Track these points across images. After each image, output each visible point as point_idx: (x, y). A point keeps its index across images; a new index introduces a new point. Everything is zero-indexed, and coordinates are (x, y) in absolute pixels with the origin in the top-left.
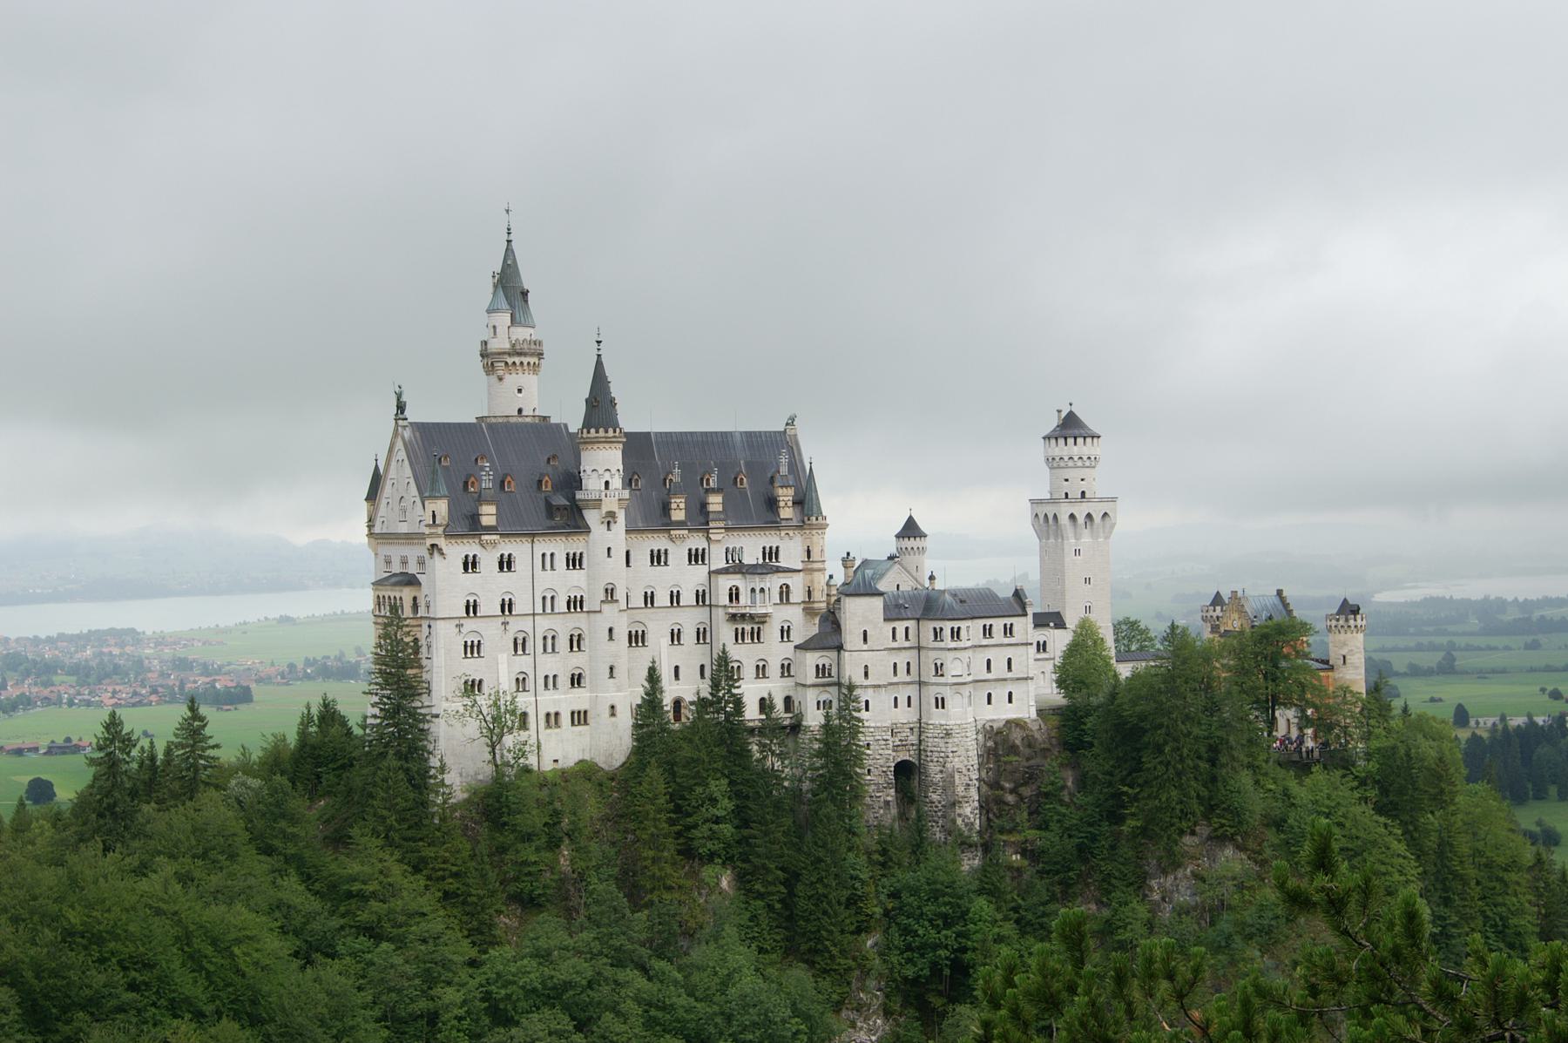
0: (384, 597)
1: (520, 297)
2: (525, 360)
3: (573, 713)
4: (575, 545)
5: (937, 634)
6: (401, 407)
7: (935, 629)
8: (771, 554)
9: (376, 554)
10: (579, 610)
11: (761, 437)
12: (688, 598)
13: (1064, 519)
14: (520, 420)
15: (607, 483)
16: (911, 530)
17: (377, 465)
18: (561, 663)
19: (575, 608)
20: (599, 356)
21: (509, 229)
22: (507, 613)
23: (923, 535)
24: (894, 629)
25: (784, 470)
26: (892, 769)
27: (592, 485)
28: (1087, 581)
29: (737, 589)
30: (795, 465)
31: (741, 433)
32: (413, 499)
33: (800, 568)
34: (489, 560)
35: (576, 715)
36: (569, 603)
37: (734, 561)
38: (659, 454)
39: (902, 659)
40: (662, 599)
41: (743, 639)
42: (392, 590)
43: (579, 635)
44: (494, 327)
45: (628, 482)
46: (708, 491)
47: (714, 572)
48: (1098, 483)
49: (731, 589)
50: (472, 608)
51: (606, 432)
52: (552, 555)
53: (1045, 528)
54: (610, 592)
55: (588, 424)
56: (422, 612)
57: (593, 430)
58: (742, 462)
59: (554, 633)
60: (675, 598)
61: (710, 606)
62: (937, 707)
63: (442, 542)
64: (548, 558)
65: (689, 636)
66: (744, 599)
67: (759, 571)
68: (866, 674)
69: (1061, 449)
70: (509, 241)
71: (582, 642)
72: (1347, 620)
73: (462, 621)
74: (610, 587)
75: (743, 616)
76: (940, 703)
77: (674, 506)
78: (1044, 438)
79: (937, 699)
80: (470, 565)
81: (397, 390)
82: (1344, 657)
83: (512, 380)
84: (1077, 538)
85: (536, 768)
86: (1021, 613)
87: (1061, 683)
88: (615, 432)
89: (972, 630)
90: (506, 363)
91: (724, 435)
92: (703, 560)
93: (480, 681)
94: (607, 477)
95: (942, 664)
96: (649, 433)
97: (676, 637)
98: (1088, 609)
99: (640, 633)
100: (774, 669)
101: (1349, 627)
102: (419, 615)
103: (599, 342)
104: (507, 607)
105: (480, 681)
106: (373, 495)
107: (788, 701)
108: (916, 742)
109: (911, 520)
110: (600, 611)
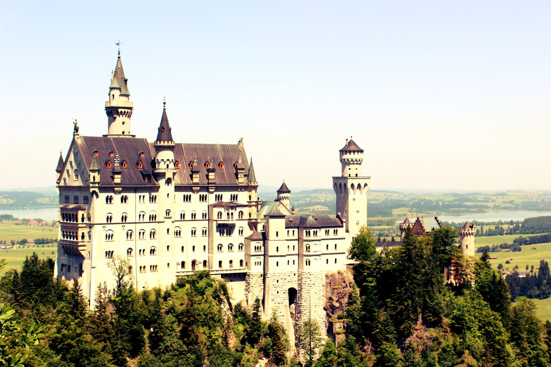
0: (66, 214)
1: (123, 82)
2: (126, 110)
3: (151, 266)
4: (153, 194)
5: (308, 234)
6: (76, 129)
7: (306, 231)
8: (234, 197)
9: (60, 195)
10: (154, 221)
11: (228, 146)
12: (199, 216)
13: (349, 186)
14: (124, 137)
15: (168, 165)
16: (283, 189)
17: (61, 156)
18: (147, 243)
19: (152, 220)
20: (164, 109)
21: (119, 52)
22: (124, 222)
23: (289, 192)
24: (288, 231)
25: (240, 161)
26: (288, 291)
27: (161, 167)
28: (358, 212)
29: (221, 213)
30: (244, 161)
31: (220, 145)
32: (82, 171)
33: (247, 204)
34: (117, 198)
35: (152, 267)
36: (150, 218)
37: (218, 200)
38: (185, 152)
39: (291, 244)
40: (188, 217)
41: (223, 235)
42: (71, 211)
43: (154, 232)
44: (113, 95)
45: (176, 164)
46: (209, 171)
47: (211, 205)
48: (361, 170)
49: (218, 213)
50: (109, 219)
51: (168, 143)
52: (144, 196)
53: (339, 189)
54: (168, 212)
55: (159, 139)
56: (86, 221)
57: (162, 142)
58: (221, 157)
59: (143, 231)
60: (194, 216)
61: (208, 220)
62: (307, 265)
63: (97, 190)
64: (142, 198)
65: (199, 233)
66: (225, 216)
67: (231, 205)
68: (277, 250)
69: (347, 156)
70: (119, 57)
71: (155, 235)
72: (469, 230)
73: (105, 225)
74: (168, 211)
75: (224, 224)
76: (308, 263)
77: (194, 176)
78: (340, 151)
79: (306, 261)
80: (109, 200)
81: (75, 122)
82: (467, 246)
83: (119, 119)
84: (354, 194)
85: (135, 290)
86: (341, 225)
87: (353, 255)
88: (172, 143)
89: (321, 233)
90: (118, 112)
91: (213, 145)
92: (206, 200)
93: (113, 252)
94: (168, 163)
95: (309, 247)
96: (181, 144)
97: (194, 233)
98: (358, 224)
99: (178, 231)
100: (235, 248)
101: (469, 233)
102: (85, 222)
103: (164, 103)
104: (124, 218)
105: (113, 252)
106: (61, 167)
107: (241, 261)
108: (297, 280)
109: (284, 186)
110: (163, 222)
